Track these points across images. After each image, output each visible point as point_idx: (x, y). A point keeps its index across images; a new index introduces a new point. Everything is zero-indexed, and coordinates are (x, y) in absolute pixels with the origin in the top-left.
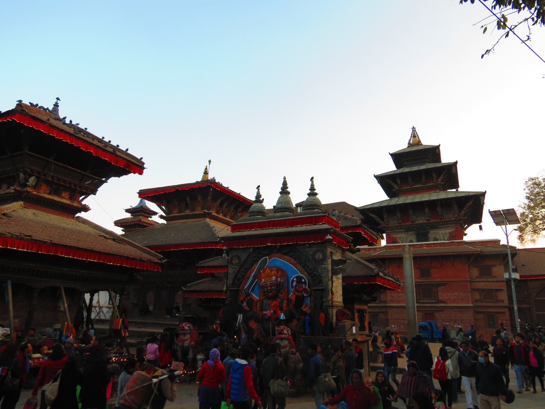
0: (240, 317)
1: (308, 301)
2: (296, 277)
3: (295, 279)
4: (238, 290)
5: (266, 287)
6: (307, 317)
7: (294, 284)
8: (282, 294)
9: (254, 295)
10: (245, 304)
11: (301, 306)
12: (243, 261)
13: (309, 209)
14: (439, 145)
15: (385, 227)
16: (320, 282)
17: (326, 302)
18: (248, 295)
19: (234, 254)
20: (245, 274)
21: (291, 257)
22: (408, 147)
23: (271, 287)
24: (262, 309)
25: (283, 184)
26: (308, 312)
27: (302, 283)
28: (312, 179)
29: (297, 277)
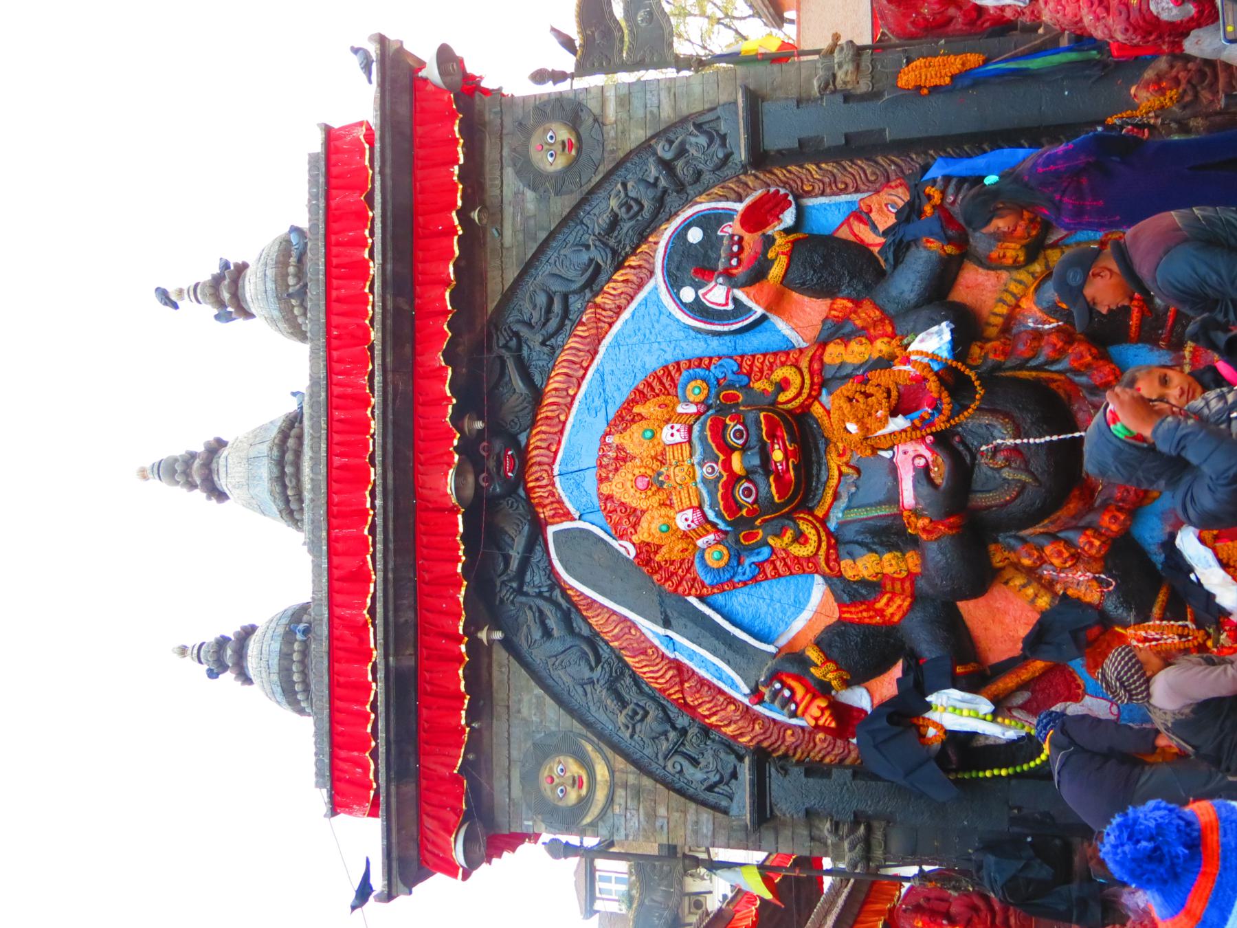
0: (955, 711)
3: (688, 294)
4: (761, 757)
5: (729, 497)
6: (936, 172)
7: (716, 294)
9: (798, 624)
10: (860, 698)
11: (861, 248)
12: (567, 722)
13: (300, 274)
16: (703, 124)
23: (728, 450)
24: (890, 534)
26: (899, 197)
28: (165, 297)
29: (674, 284)
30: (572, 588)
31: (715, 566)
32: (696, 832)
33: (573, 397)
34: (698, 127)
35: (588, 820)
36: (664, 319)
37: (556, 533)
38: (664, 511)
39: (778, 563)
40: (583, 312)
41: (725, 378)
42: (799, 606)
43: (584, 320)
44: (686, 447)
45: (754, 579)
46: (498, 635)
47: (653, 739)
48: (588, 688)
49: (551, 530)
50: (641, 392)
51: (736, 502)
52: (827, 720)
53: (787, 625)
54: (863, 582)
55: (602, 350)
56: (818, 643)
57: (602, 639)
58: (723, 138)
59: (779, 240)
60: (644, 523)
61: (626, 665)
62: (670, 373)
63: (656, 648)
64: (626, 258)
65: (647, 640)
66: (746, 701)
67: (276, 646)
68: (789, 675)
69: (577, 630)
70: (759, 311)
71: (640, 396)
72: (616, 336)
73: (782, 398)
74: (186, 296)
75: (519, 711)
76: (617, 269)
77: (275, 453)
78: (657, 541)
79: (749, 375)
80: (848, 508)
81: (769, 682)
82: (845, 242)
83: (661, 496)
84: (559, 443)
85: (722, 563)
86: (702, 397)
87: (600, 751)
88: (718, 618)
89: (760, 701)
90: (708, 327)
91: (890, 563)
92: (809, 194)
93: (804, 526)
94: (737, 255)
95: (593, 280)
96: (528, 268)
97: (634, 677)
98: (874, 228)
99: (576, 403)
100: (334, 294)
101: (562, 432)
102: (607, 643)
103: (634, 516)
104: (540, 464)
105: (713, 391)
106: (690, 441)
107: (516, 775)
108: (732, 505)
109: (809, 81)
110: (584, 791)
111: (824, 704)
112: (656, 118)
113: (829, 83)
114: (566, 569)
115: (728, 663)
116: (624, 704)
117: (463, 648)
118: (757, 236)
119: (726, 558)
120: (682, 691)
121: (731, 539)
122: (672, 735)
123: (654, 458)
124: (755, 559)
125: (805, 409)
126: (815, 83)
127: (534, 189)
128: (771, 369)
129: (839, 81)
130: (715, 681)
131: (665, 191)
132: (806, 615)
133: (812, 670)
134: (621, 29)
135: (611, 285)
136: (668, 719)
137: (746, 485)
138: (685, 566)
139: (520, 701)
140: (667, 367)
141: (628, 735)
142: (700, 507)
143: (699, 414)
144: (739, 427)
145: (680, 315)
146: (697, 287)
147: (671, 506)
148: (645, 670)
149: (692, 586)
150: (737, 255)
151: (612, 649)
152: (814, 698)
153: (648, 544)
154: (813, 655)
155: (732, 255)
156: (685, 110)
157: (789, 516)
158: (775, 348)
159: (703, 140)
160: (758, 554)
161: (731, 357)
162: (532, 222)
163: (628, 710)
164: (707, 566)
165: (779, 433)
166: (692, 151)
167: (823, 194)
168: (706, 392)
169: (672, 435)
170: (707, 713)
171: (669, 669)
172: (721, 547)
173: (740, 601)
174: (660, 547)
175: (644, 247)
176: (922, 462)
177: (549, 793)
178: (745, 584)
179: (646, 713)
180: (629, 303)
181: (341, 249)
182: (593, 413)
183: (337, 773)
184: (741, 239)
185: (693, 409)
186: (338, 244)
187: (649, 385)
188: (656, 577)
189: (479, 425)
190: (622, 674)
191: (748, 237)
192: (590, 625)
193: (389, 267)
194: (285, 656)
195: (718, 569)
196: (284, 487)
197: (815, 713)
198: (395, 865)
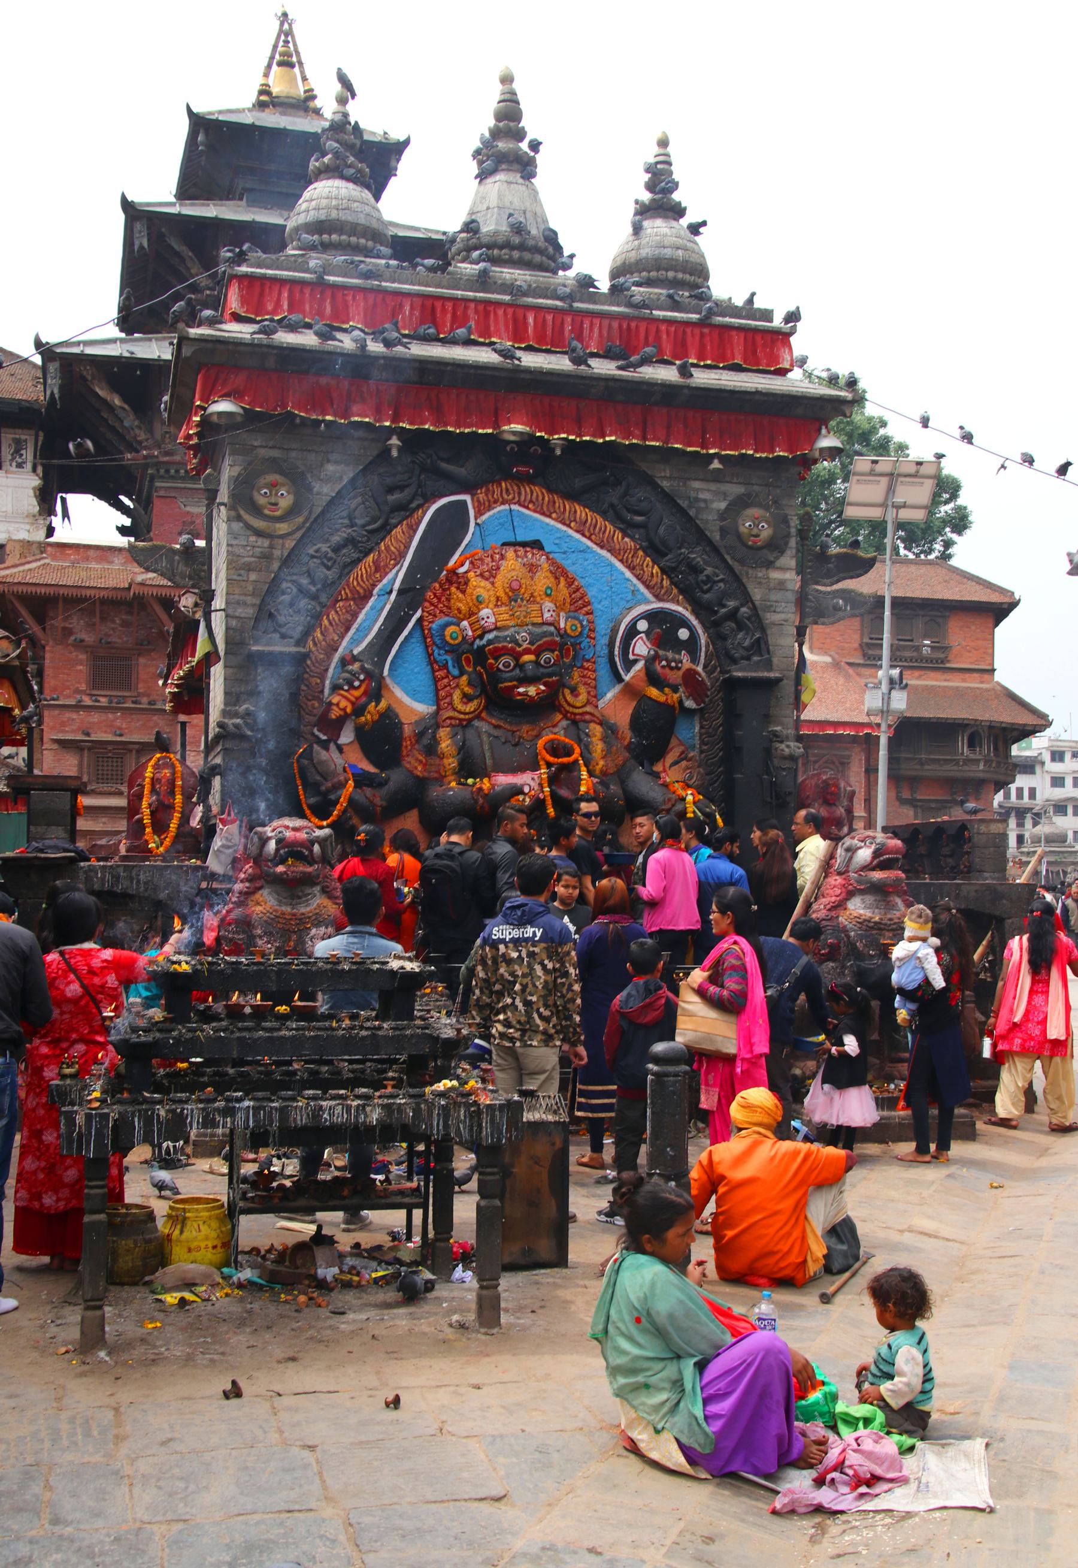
1: (689, 732)
3: (643, 625)
5: (504, 651)
7: (641, 648)
8: (574, 691)
9: (398, 692)
10: (347, 736)
14: (407, 143)
15: (158, 465)
16: (760, 647)
17: (787, 738)
19: (262, 452)
21: (604, 514)
22: (261, 105)
23: (538, 653)
25: (500, 116)
27: (678, 645)
29: (651, 617)
30: (424, 513)
32: (238, 603)
33: (569, 526)
34: (758, 640)
35: (242, 513)
36: (623, 604)
37: (465, 502)
38: (493, 599)
40: (632, 538)
42: (413, 695)
43: (627, 539)
44: (540, 620)
45: (431, 661)
46: (395, 453)
47: (308, 571)
48: (346, 521)
49: (467, 498)
52: (335, 713)
53: (398, 684)
54: (435, 742)
55: (604, 553)
56: (389, 708)
58: (748, 658)
59: (676, 696)
60: (483, 583)
61: (367, 554)
64: (669, 577)
65: (386, 574)
66: (341, 650)
67: (362, 220)
70: (627, 678)
71: (570, 582)
72: (611, 565)
73: (567, 692)
74: (662, 151)
75: (328, 461)
76: (663, 571)
77: (531, 243)
78: (469, 591)
79: (582, 667)
80: (490, 735)
81: (363, 669)
82: (669, 742)
83: (505, 599)
84: (535, 511)
85: (448, 638)
87: (298, 529)
89: (344, 662)
91: (451, 763)
92: (702, 718)
93: (476, 702)
94: (669, 666)
95: (655, 550)
96: (668, 499)
97: (359, 560)
98: (675, 763)
99: (564, 528)
100: (663, 328)
101: (543, 514)
102: (383, 539)
103: (490, 575)
104: (520, 494)
106: (543, 624)
107: (275, 453)
108: (498, 653)
109: (781, 724)
110: (266, 512)
111: (349, 710)
112: (768, 609)
113: (777, 737)
116: (336, 549)
117: (387, 424)
118: (679, 681)
120: (347, 599)
121: (466, 646)
122: (313, 589)
123: (532, 595)
124: (450, 663)
126: (779, 728)
127: (726, 509)
128: (585, 684)
129: (778, 745)
130: (355, 626)
131: (716, 612)
132: (407, 700)
134: (832, 584)
139: (336, 462)
140: (589, 603)
141: (311, 551)
142: (497, 628)
143: (558, 629)
146: (647, 633)
147: (496, 606)
150: (669, 666)
151: (378, 544)
152: (353, 704)
153: (466, 584)
154: (383, 704)
155: (668, 661)
156: (769, 632)
157: (484, 692)
159: (747, 643)
162: (702, 505)
163: (331, 554)
166: (740, 635)
167: (702, 727)
173: (417, 651)
174: (464, 592)
175: (675, 591)
176: (526, 789)
177: (262, 481)
178: (430, 655)
179: (329, 568)
180: (637, 577)
181: (697, 338)
183: (268, 284)
184: (679, 669)
185: (562, 625)
186: (702, 335)
187: (577, 590)
188: (437, 585)
189: (558, 452)
191: (681, 673)
193: (686, 391)
194: (354, 229)
196: (501, 248)
197: (341, 703)
198: (210, 346)
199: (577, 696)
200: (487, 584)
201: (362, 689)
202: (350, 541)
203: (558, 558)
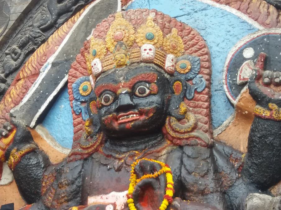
2: (253, 44)
3: (249, 53)
12: (14, 18)
18: (27, 137)
20: (23, 62)
30: (84, 10)
31: (80, 88)
39: (81, 125)
41: (193, 84)
45: (74, 112)
50: (189, 33)
51: (101, 94)
56: (34, 151)
57: (55, 31)
62: (200, 49)
63: (46, 61)
68: (16, 134)
69: (61, 17)
70: (235, 102)
72: (230, 14)
81: (12, 123)
83: (112, 49)
86: (178, 70)
88: (55, 93)
90: (225, 69)
102: (53, 34)
105: (183, 78)
114: (94, 7)
115: (29, 101)
116: (22, 47)
119: (84, 94)
120: (24, 78)
124: (83, 112)
125: (165, 136)
133: (16, 148)
135: (266, 5)
136: (11, 73)
137: (111, 97)
138: (83, 71)
141: (7, 51)
144: (148, 91)
145: (234, 50)
148: (36, 57)
149: (73, 77)
151: (49, 37)
158: (214, 115)
160: (86, 113)
161: (208, 86)
164: (81, 83)
165: (143, 117)
168: (182, 72)
169: (145, 50)
170: (11, 93)
171: (35, 69)
172: (90, 90)
178: (72, 107)
179: (15, 60)
182: (183, 7)
185: (168, 64)
190: (35, 44)
192: (63, 24)
195: (79, 90)
199: (183, 123)
200: (100, 41)
201: (11, 136)
202: (29, 40)
203: (183, 19)
